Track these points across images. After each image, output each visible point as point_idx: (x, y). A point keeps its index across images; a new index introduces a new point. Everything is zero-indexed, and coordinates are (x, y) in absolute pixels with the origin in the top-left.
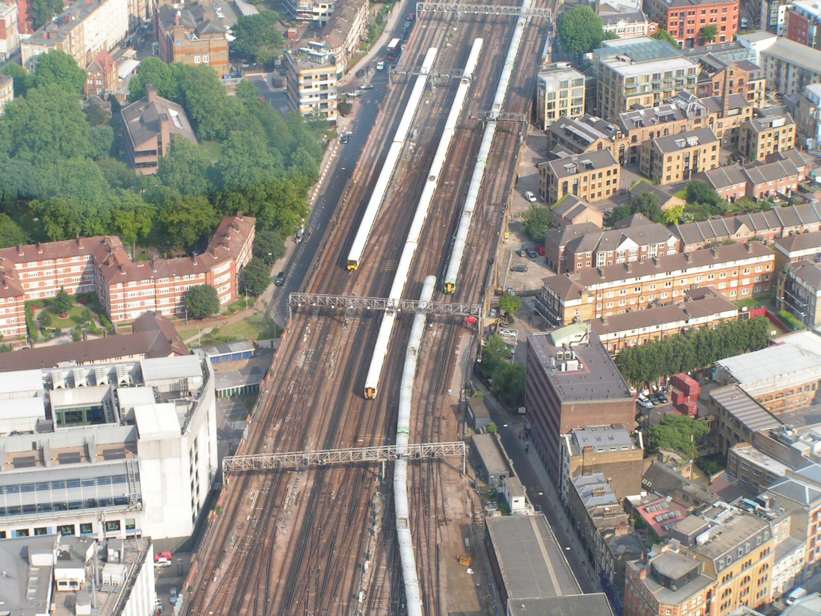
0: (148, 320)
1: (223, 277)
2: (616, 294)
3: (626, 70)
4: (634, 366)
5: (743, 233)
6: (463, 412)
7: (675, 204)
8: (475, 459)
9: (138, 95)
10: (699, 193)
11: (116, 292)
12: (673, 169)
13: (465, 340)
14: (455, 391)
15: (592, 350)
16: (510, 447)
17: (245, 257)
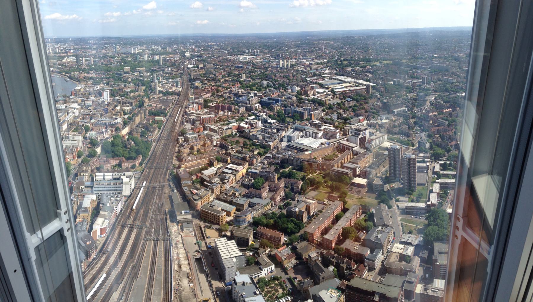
0: (127, 168)
1: (137, 163)
2: (188, 164)
3: (189, 136)
4: (191, 173)
5: (204, 156)
6: (169, 180)
7: (195, 153)
8: (170, 185)
9: (128, 140)
10: (198, 151)
11: (123, 164)
12: (195, 148)
13: (169, 171)
14: (167, 177)
15: (185, 170)
16: (174, 184)
17: (140, 160)
